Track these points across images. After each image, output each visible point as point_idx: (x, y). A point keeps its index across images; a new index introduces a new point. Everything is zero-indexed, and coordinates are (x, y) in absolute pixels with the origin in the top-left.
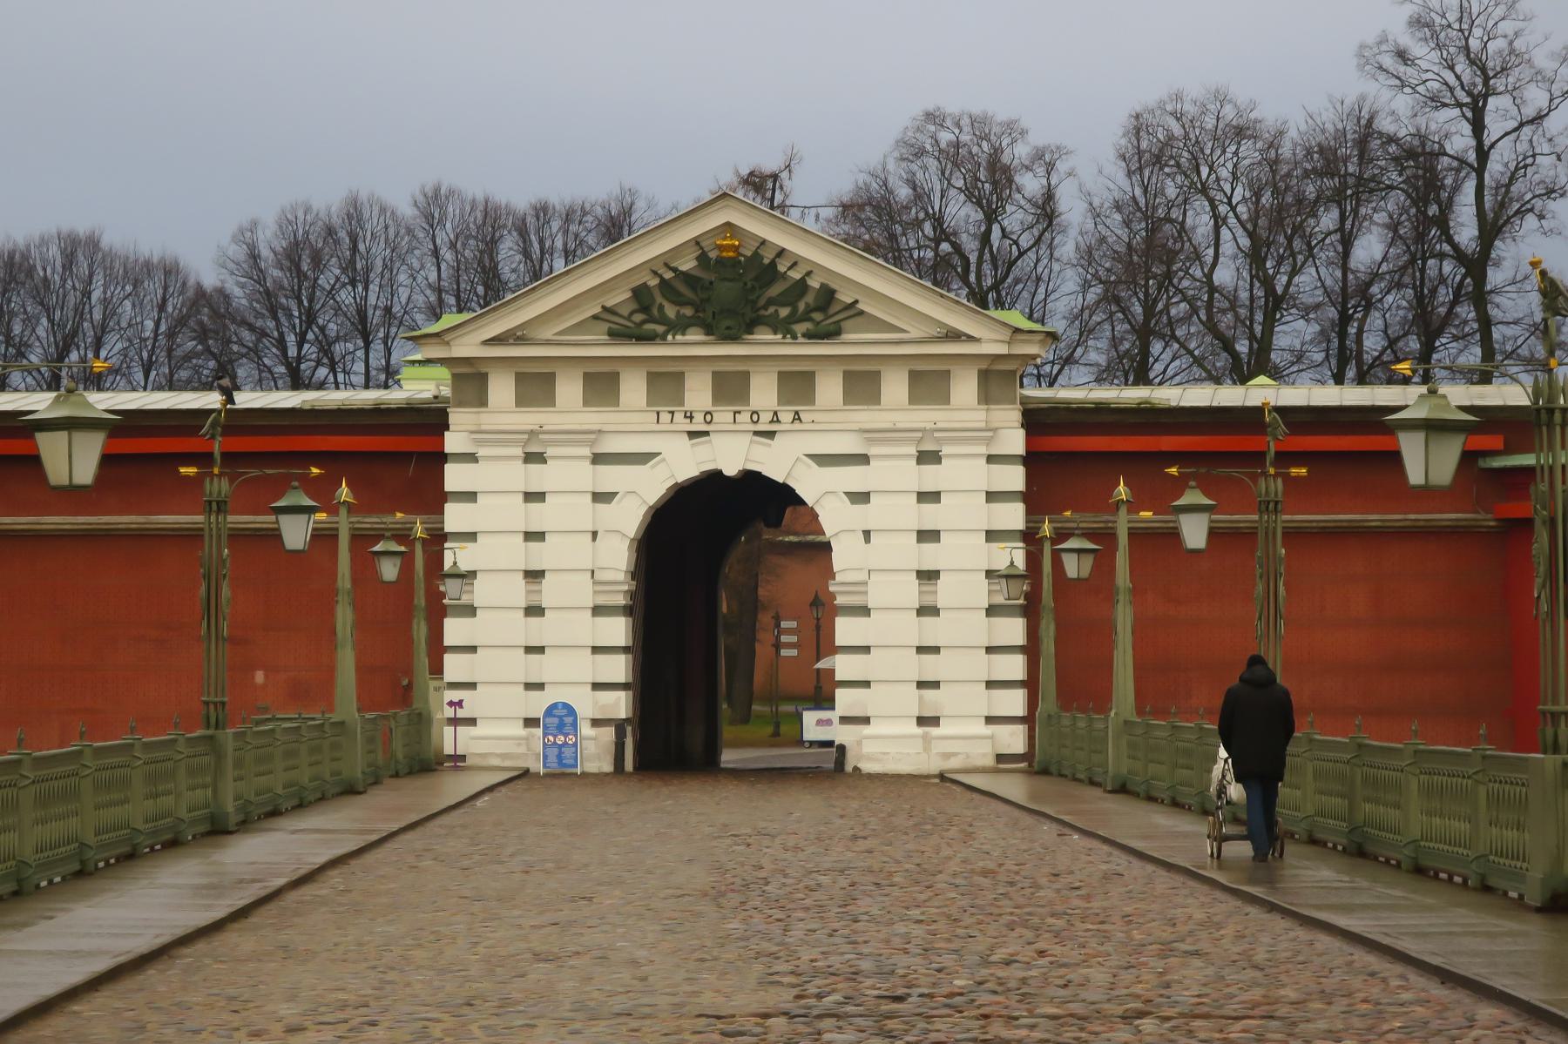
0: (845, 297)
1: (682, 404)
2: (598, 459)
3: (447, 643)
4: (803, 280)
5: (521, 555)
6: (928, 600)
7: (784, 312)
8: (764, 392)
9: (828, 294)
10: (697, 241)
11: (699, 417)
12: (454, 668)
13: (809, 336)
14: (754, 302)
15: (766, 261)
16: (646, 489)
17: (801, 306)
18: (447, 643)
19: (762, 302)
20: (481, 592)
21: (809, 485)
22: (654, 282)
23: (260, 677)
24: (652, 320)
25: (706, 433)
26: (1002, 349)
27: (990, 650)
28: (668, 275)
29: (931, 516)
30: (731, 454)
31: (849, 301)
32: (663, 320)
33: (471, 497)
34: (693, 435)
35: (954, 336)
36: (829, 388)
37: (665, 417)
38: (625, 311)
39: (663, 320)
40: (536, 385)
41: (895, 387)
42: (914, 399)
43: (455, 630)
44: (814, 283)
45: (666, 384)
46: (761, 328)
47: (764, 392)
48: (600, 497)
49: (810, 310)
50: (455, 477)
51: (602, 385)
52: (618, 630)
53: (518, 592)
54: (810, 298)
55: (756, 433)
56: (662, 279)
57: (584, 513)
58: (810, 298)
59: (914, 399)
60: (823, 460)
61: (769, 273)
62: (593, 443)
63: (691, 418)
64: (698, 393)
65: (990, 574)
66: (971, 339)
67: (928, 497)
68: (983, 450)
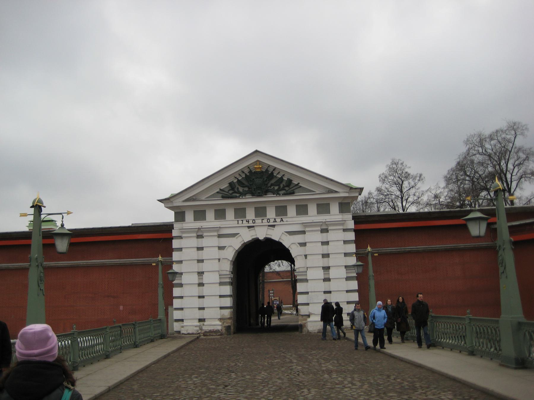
0: (295, 182)
1: (245, 218)
2: (220, 236)
3: (174, 296)
4: (282, 178)
5: (196, 267)
6: (327, 276)
7: (276, 188)
8: (271, 213)
9: (290, 181)
10: (248, 167)
11: (251, 222)
12: (176, 303)
13: (285, 194)
14: (267, 184)
15: (270, 172)
16: (235, 245)
17: (282, 186)
18: (174, 296)
19: (269, 185)
20: (185, 279)
21: (287, 242)
22: (235, 181)
23: (121, 308)
24: (235, 192)
25: (253, 227)
26: (346, 195)
27: (347, 291)
28: (240, 178)
29: (325, 249)
30: (261, 233)
31: (296, 183)
32: (239, 192)
33: (180, 249)
34: (249, 227)
35: (331, 191)
36: (292, 211)
37: (240, 222)
38: (227, 190)
39: (239, 192)
40: (200, 215)
41: (312, 209)
42: (319, 212)
43: (176, 292)
44: (285, 178)
45: (240, 213)
46: (269, 193)
47: (271, 213)
48: (221, 248)
49: (284, 187)
50: (176, 244)
51: (220, 214)
52: (227, 290)
53: (195, 279)
54: (284, 183)
55: (269, 226)
56: (238, 180)
57: (215, 253)
58: (284, 183)
59: (319, 212)
60: (291, 233)
61: (271, 176)
62: (218, 231)
63: (248, 222)
64: (250, 214)
65: (346, 267)
66: (336, 192)
67: (326, 243)
68: (341, 227)
